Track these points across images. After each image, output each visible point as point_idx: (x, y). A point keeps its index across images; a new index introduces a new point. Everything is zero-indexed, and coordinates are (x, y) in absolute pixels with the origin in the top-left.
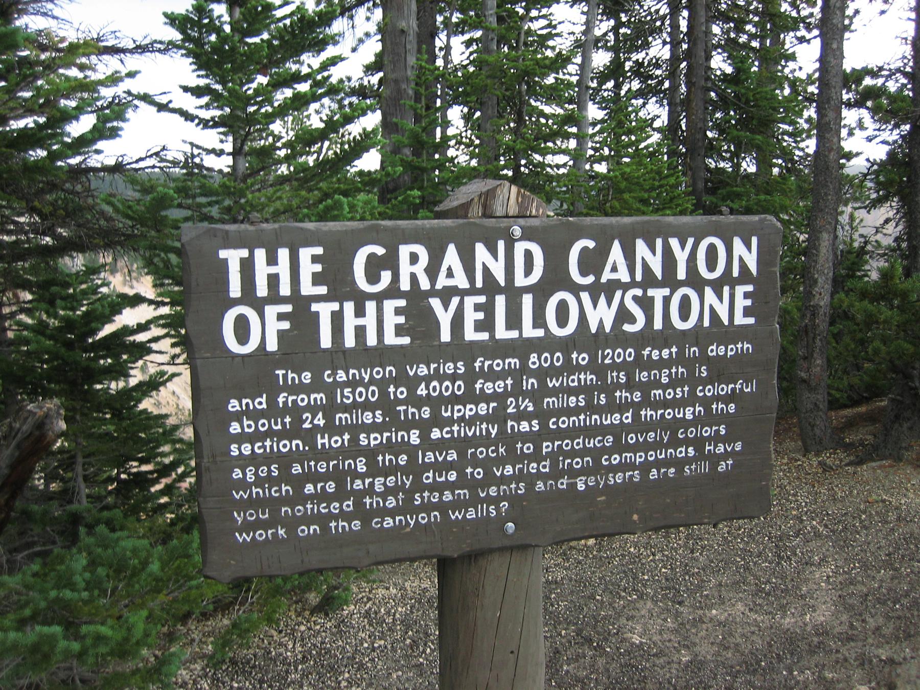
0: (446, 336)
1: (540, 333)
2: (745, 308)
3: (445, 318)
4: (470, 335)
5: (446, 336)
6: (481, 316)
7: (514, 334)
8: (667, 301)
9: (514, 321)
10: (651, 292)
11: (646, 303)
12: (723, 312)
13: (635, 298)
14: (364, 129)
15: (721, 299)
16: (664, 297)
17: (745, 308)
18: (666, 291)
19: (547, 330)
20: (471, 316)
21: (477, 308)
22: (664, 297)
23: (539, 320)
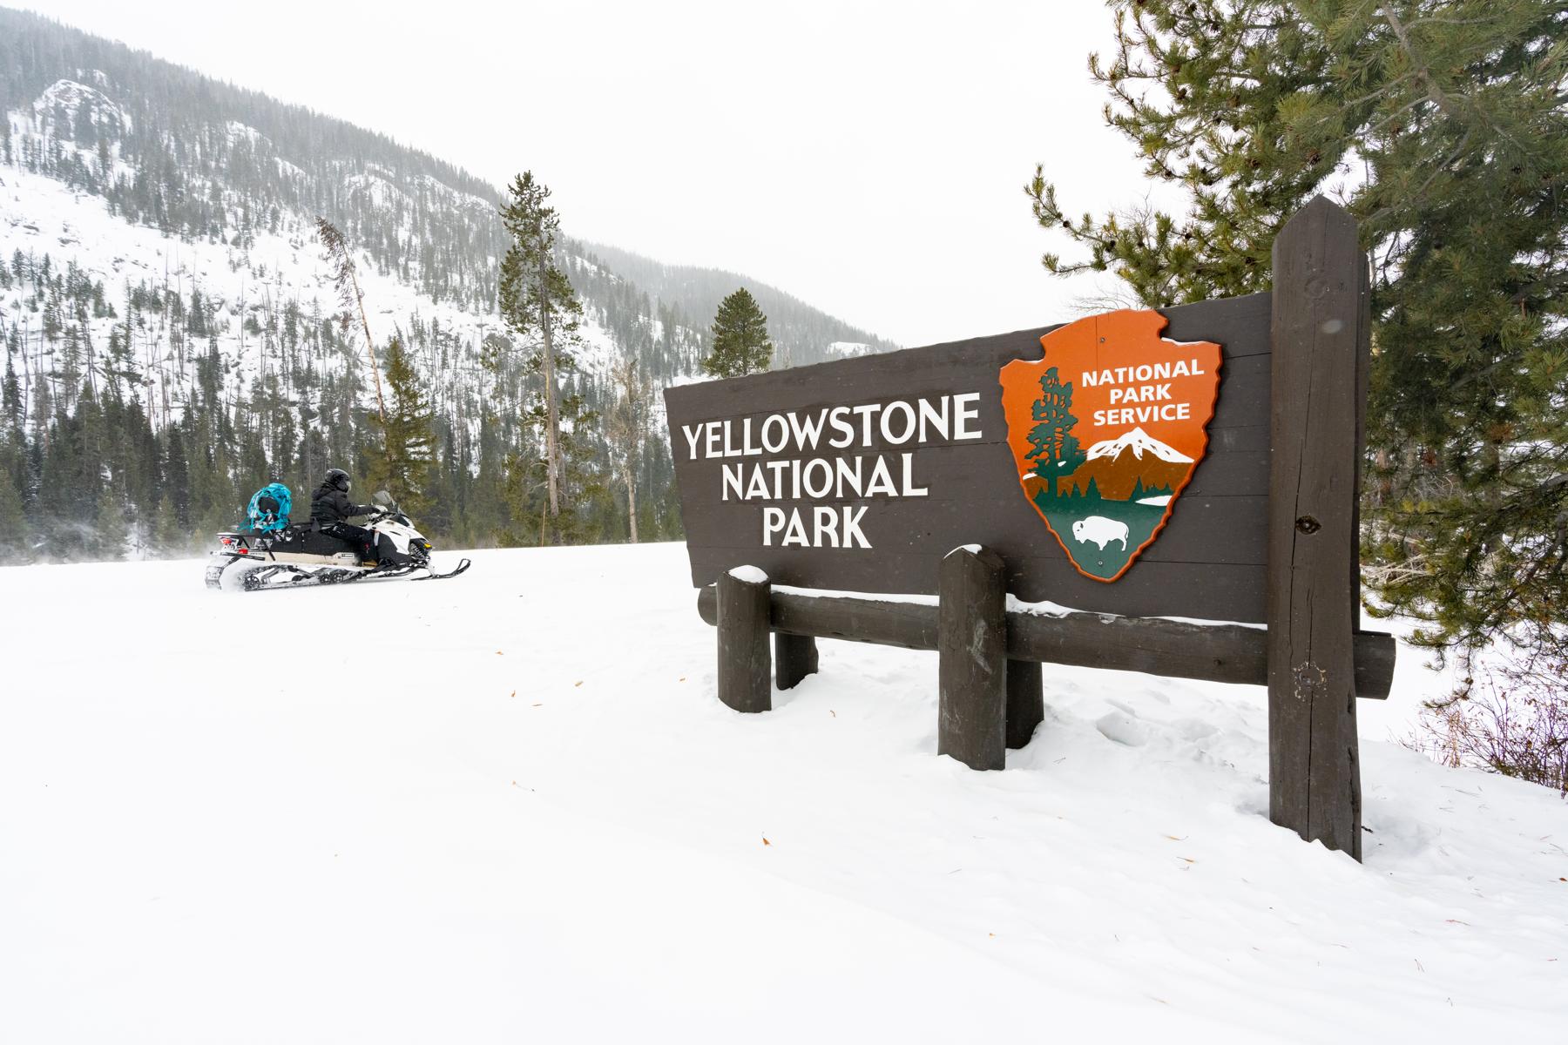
0: (693, 456)
1: (759, 451)
2: (967, 420)
3: (693, 442)
4: (710, 454)
5: (693, 456)
6: (717, 438)
7: (738, 453)
8: (876, 417)
9: (737, 443)
10: (857, 410)
11: (856, 421)
12: (942, 426)
14: (435, 301)
15: (939, 411)
17: (967, 420)
18: (877, 407)
19: (764, 450)
20: (711, 438)
21: (715, 431)
23: (756, 442)
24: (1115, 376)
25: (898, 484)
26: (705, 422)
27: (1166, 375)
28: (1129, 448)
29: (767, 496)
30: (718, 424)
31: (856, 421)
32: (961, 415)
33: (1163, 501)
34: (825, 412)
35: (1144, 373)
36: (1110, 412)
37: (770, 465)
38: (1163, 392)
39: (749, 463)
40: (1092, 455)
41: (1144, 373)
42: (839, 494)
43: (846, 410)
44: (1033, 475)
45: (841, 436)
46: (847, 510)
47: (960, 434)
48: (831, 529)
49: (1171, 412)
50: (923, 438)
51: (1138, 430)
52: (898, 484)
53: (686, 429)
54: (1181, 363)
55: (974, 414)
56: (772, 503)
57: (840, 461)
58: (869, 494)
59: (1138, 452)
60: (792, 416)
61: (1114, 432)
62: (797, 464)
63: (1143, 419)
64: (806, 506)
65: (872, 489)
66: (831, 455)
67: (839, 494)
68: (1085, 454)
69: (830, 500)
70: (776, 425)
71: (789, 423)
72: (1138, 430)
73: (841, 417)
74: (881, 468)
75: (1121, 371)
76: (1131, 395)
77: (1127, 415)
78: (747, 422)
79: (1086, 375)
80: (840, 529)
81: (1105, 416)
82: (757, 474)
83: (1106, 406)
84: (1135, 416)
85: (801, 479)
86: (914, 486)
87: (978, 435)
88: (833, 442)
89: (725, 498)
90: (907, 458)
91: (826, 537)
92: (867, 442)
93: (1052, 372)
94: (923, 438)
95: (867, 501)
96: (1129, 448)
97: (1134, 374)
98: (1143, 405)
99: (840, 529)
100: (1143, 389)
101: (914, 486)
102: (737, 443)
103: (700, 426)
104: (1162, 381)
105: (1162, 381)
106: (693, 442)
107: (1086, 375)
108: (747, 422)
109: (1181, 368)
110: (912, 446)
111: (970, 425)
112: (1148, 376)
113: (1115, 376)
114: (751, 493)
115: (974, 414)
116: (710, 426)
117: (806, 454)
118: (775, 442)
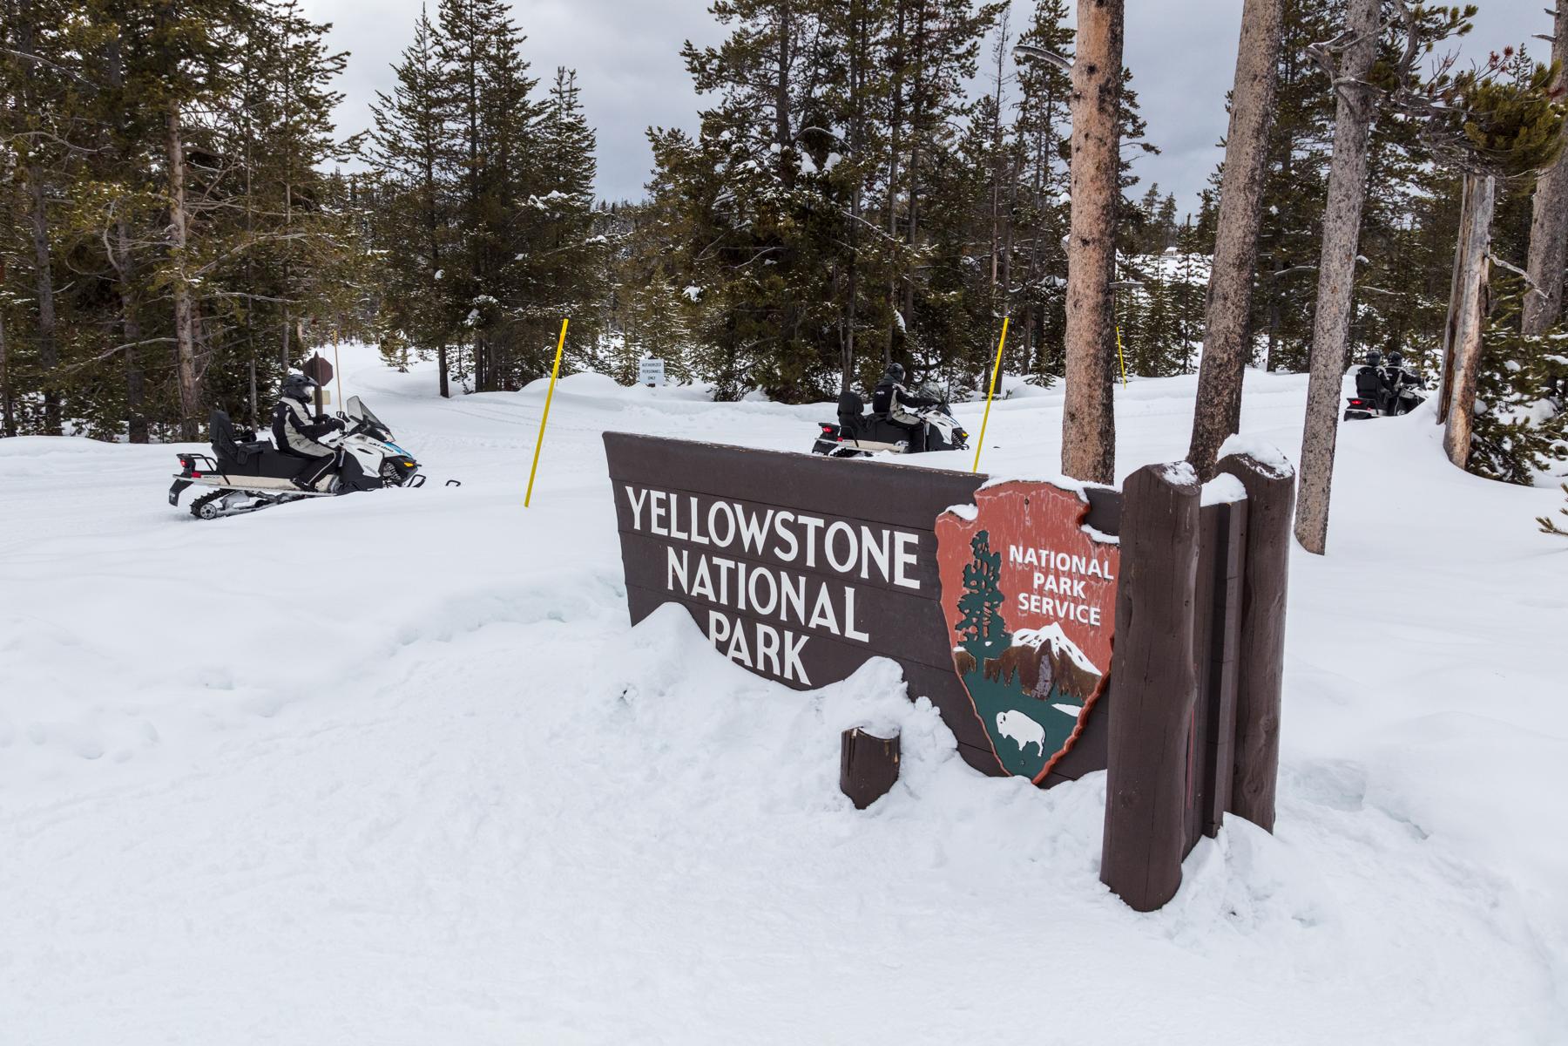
0: (637, 526)
3: (637, 509)
4: (655, 529)
5: (637, 526)
6: (662, 512)
7: (684, 536)
8: (820, 534)
9: (684, 525)
10: (802, 519)
11: (800, 531)
13: (785, 523)
16: (817, 528)
18: (821, 523)
20: (656, 511)
22: (817, 528)
23: (703, 531)
24: (1039, 558)
25: (841, 624)
26: (650, 487)
27: (1083, 571)
28: (1048, 641)
29: (712, 598)
30: (662, 495)
31: (800, 531)
32: (902, 558)
33: (1074, 711)
34: (770, 513)
35: (1063, 562)
36: (1033, 598)
37: (716, 561)
38: (1078, 588)
39: (696, 551)
40: (1016, 642)
41: (1063, 562)
42: (783, 617)
43: (790, 517)
44: (962, 649)
45: (786, 548)
46: (789, 635)
47: (900, 580)
48: (772, 652)
49: (1085, 614)
50: (865, 574)
51: (1056, 625)
52: (841, 624)
53: (630, 490)
54: (1095, 561)
55: (912, 559)
56: (718, 607)
57: (784, 575)
58: (812, 625)
59: (1055, 649)
60: (738, 507)
61: (1037, 621)
62: (742, 567)
63: (1061, 614)
64: (750, 619)
65: (815, 621)
66: (777, 566)
67: (783, 617)
68: (1009, 637)
69: (772, 620)
70: (721, 512)
71: (736, 513)
72: (1056, 625)
73: (785, 523)
74: (824, 598)
75: (1044, 553)
76: (1051, 584)
77: (1048, 605)
78: (694, 501)
79: (1013, 548)
80: (781, 654)
81: (1028, 599)
82: (703, 569)
83: (1030, 591)
84: (1054, 608)
85: (747, 591)
86: (856, 629)
87: (915, 584)
88: (777, 551)
89: (670, 587)
90: (850, 592)
91: (767, 659)
92: (811, 562)
93: (982, 535)
94: (865, 574)
95: (805, 630)
96: (1048, 641)
97: (1056, 559)
98: (1063, 598)
99: (781, 654)
100: (1062, 580)
101: (856, 629)
102: (684, 525)
103: (644, 492)
104: (1082, 578)
105: (1082, 578)
106: (637, 509)
107: (1013, 548)
108: (694, 501)
109: (1094, 567)
110: (852, 578)
111: (910, 571)
112: (1066, 568)
113: (1039, 558)
114: (696, 590)
115: (912, 559)
116: (656, 495)
117: (752, 559)
118: (722, 534)
